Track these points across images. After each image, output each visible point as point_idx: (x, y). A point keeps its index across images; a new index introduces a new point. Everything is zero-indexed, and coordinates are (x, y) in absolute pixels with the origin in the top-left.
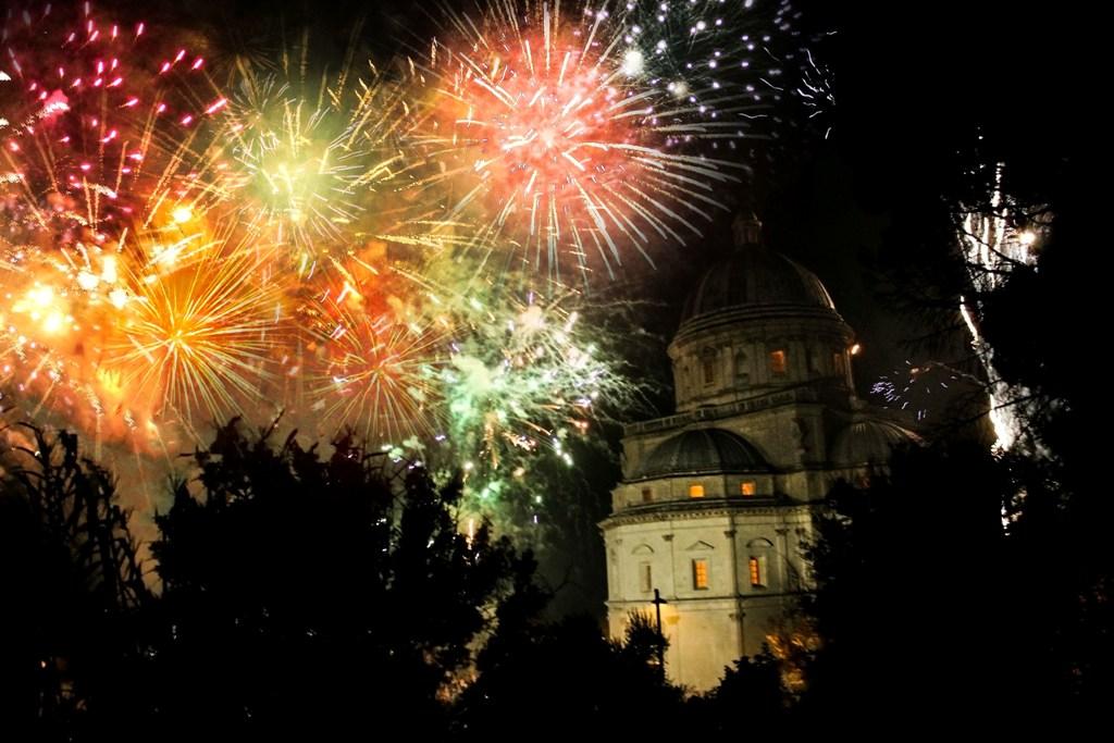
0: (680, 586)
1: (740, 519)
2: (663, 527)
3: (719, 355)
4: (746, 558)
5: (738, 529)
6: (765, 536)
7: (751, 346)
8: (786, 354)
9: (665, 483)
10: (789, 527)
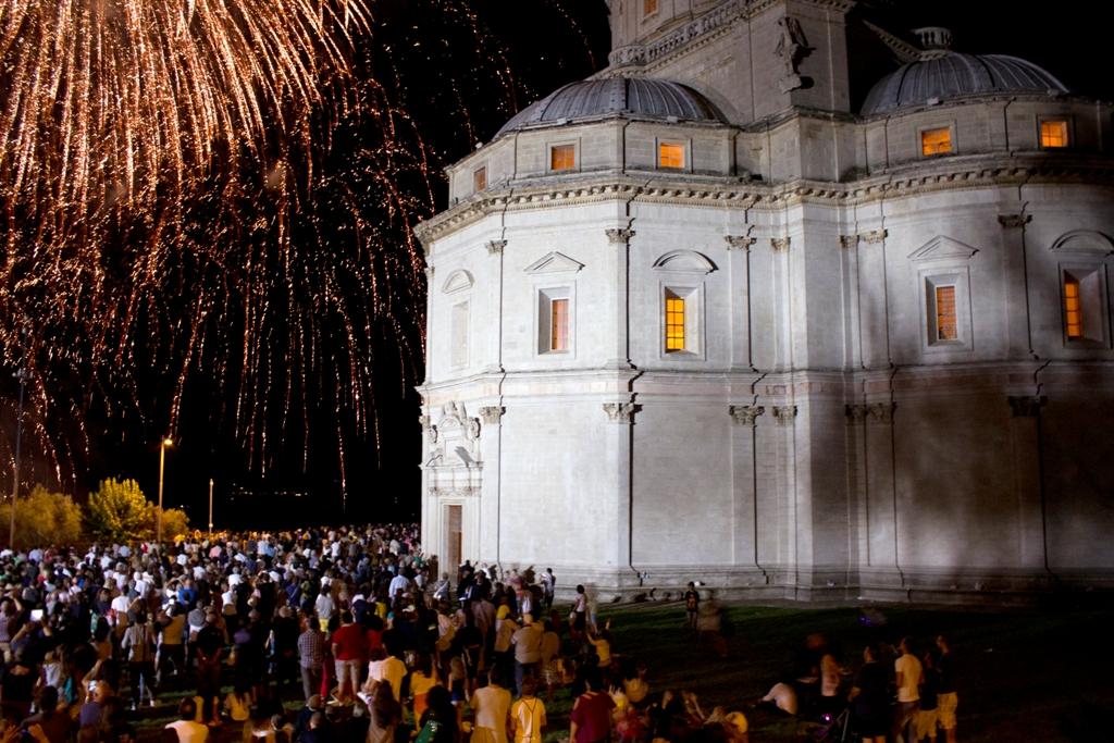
0: (513, 345)
1: (644, 209)
2: (488, 227)
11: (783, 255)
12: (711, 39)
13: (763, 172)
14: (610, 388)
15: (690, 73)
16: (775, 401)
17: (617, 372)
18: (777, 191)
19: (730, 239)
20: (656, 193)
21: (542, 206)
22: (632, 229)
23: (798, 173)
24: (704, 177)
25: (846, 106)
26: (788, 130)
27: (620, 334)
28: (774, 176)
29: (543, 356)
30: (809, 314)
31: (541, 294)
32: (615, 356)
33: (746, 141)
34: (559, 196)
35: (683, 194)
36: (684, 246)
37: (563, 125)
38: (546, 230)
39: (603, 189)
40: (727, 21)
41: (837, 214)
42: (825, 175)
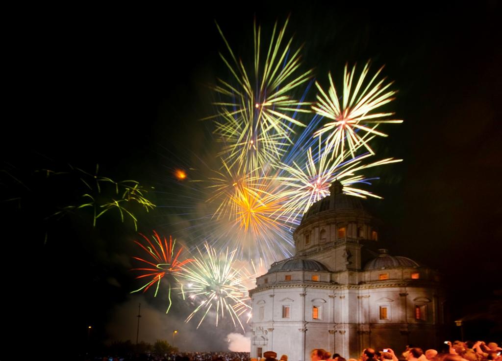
1: (309, 290)
2: (271, 291)
3: (313, 232)
4: (311, 307)
7: (328, 227)
11: (343, 300)
13: (338, 282)
14: (301, 326)
16: (340, 330)
18: (342, 286)
19: (330, 296)
23: (348, 283)
24: (323, 283)
25: (360, 268)
28: (341, 283)
29: (284, 319)
30: (349, 312)
31: (283, 307)
33: (334, 275)
41: (357, 291)
42: (354, 283)
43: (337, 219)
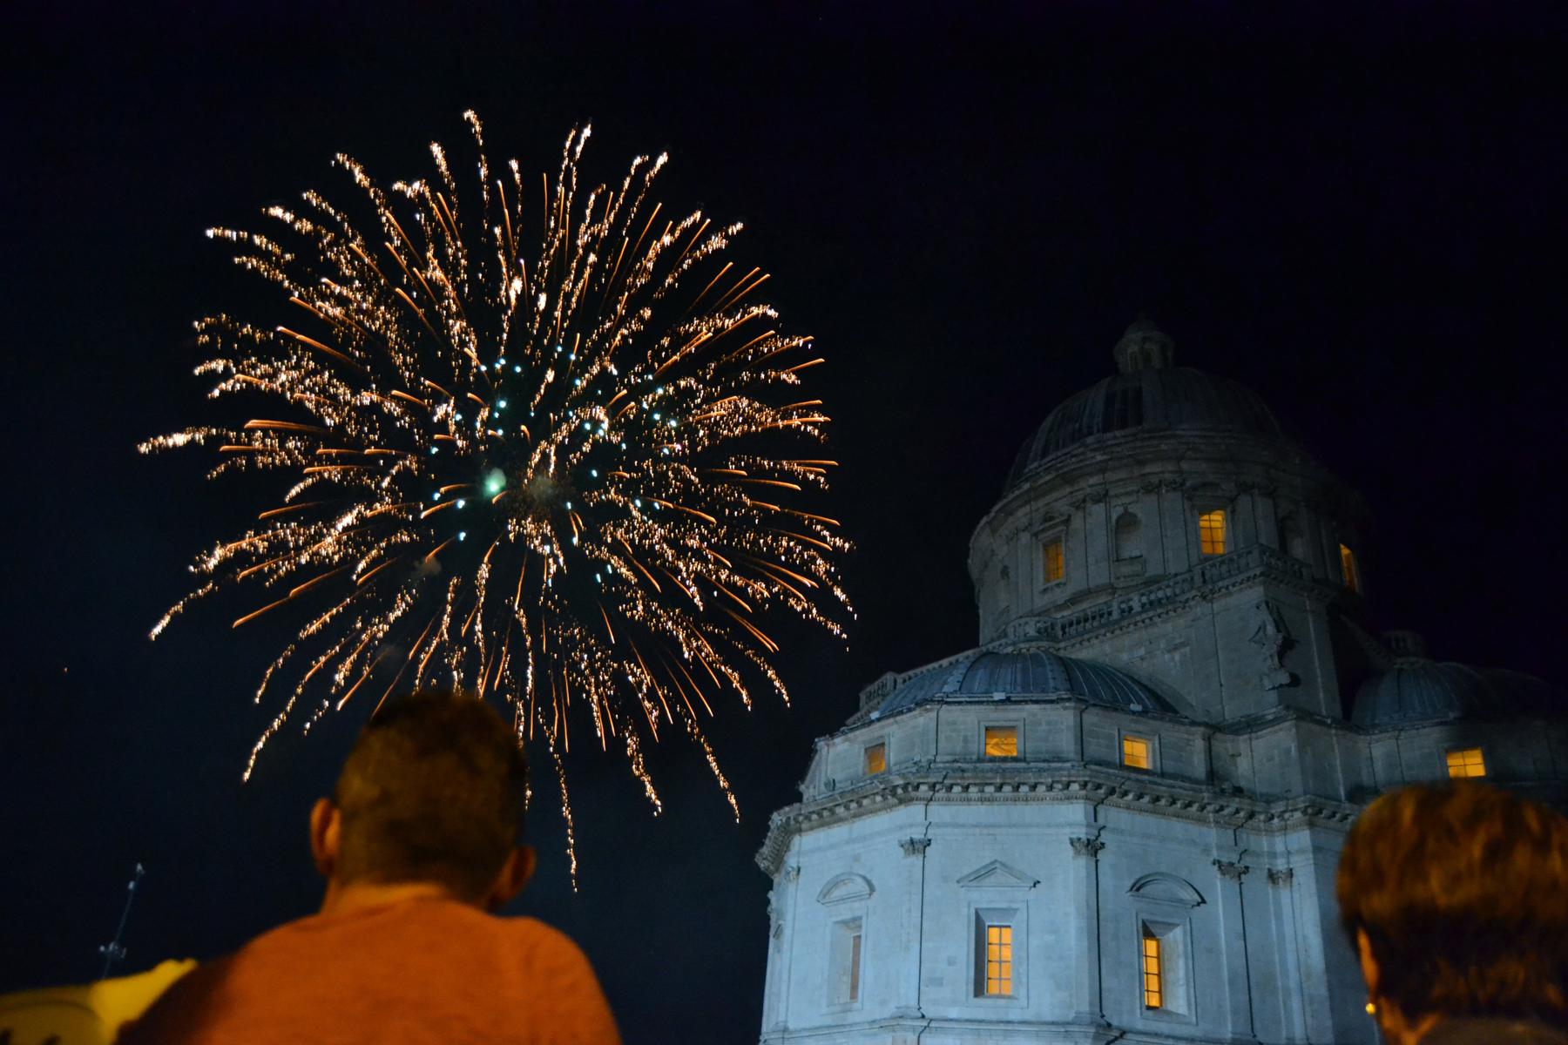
0: (939, 982)
1: (1116, 816)
2: (909, 818)
3: (1077, 522)
4: (1131, 927)
5: (1105, 837)
6: (1184, 874)
7: (1150, 501)
8: (1232, 520)
9: (921, 720)
10: (1247, 861)
11: (1285, 894)
12: (1156, 619)
13: (1243, 784)
15: (1125, 657)
17: (1093, 1030)
18: (1278, 808)
20: (1130, 796)
21: (982, 800)
22: (1101, 839)
26: (1281, 734)
27: (1091, 977)
29: (980, 1001)
32: (1085, 1008)
33: (1224, 744)
34: (1007, 789)
35: (1163, 802)
36: (1163, 869)
37: (1002, 702)
38: (985, 831)
39: (1067, 786)
40: (1183, 598)
43: (1185, 466)
